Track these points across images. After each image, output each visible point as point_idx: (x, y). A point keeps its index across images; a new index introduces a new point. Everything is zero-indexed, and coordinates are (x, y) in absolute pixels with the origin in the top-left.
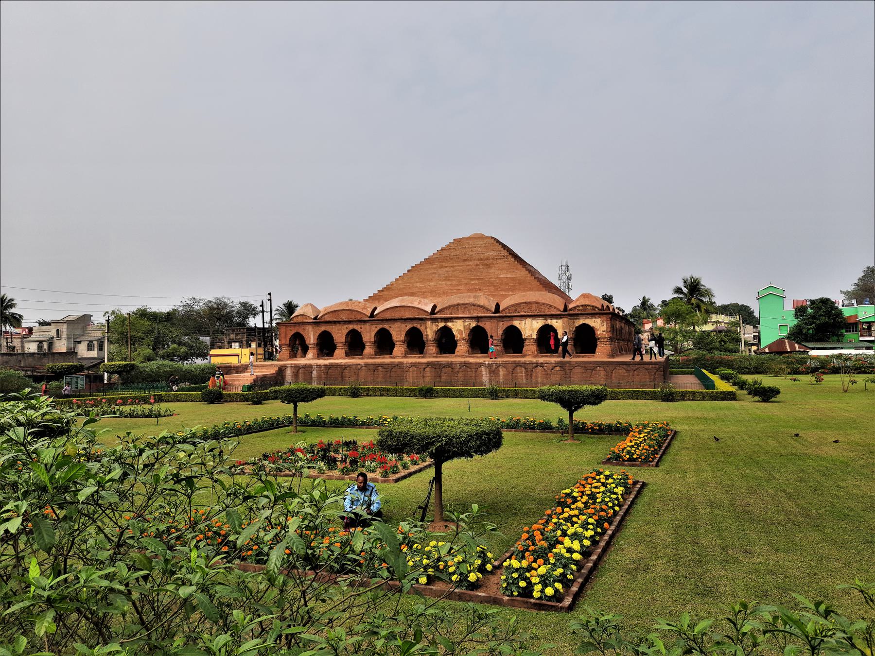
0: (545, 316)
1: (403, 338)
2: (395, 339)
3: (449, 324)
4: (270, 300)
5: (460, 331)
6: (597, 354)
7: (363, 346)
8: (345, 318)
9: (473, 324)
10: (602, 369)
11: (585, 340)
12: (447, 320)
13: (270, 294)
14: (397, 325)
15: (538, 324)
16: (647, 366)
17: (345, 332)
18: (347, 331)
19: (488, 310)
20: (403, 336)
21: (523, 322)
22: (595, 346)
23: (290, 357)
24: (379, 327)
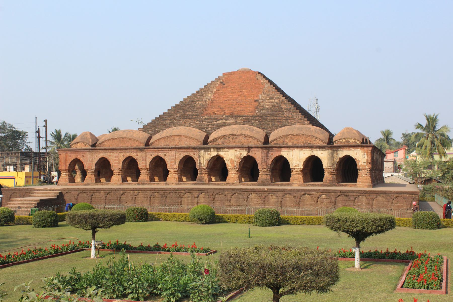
0: (311, 147)
1: (177, 166)
2: (169, 166)
3: (222, 154)
4: (45, 126)
5: (232, 161)
6: (358, 183)
7: (138, 173)
8: (121, 145)
9: (244, 153)
10: (364, 198)
11: (347, 169)
12: (218, 149)
13: (45, 121)
14: (172, 153)
15: (305, 154)
16: (405, 196)
17: (122, 159)
18: (123, 158)
19: (258, 140)
20: (177, 164)
21: (291, 153)
22: (357, 176)
23: (70, 182)
24: (154, 155)
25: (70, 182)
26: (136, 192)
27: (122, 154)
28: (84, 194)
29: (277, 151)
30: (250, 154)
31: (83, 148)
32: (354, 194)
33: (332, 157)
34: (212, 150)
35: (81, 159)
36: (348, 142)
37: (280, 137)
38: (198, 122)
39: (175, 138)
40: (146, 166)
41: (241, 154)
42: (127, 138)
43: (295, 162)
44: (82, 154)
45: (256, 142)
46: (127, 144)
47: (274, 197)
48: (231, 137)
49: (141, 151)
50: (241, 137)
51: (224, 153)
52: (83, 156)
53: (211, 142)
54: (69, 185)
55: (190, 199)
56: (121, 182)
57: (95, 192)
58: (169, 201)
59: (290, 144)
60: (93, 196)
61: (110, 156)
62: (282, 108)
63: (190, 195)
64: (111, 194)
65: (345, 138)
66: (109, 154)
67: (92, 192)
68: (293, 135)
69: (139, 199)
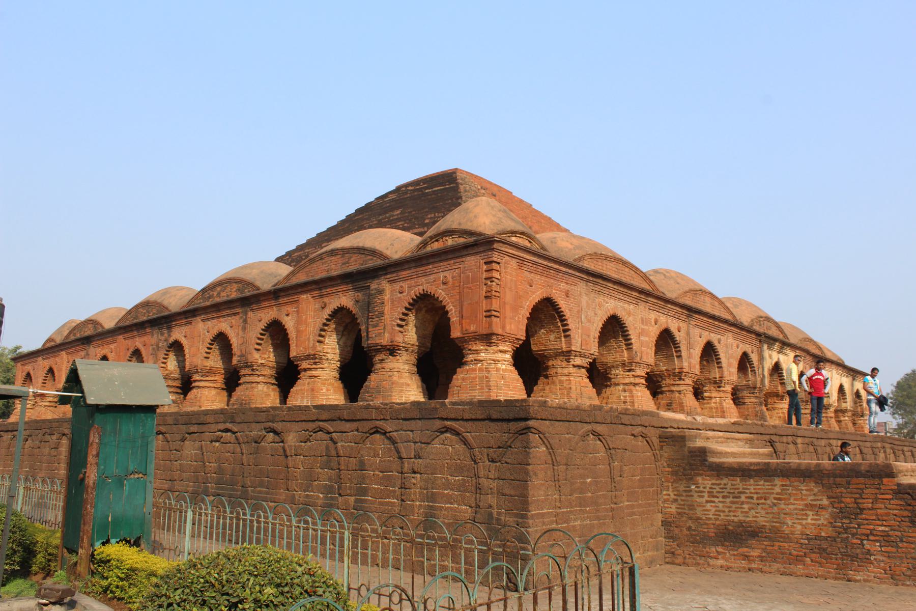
3: (782, 358)
24: (707, 336)
27: (653, 315)
33: (852, 390)
35: (562, 304)
40: (694, 367)
44: (563, 286)
49: (689, 316)
61: (629, 314)
66: (626, 305)
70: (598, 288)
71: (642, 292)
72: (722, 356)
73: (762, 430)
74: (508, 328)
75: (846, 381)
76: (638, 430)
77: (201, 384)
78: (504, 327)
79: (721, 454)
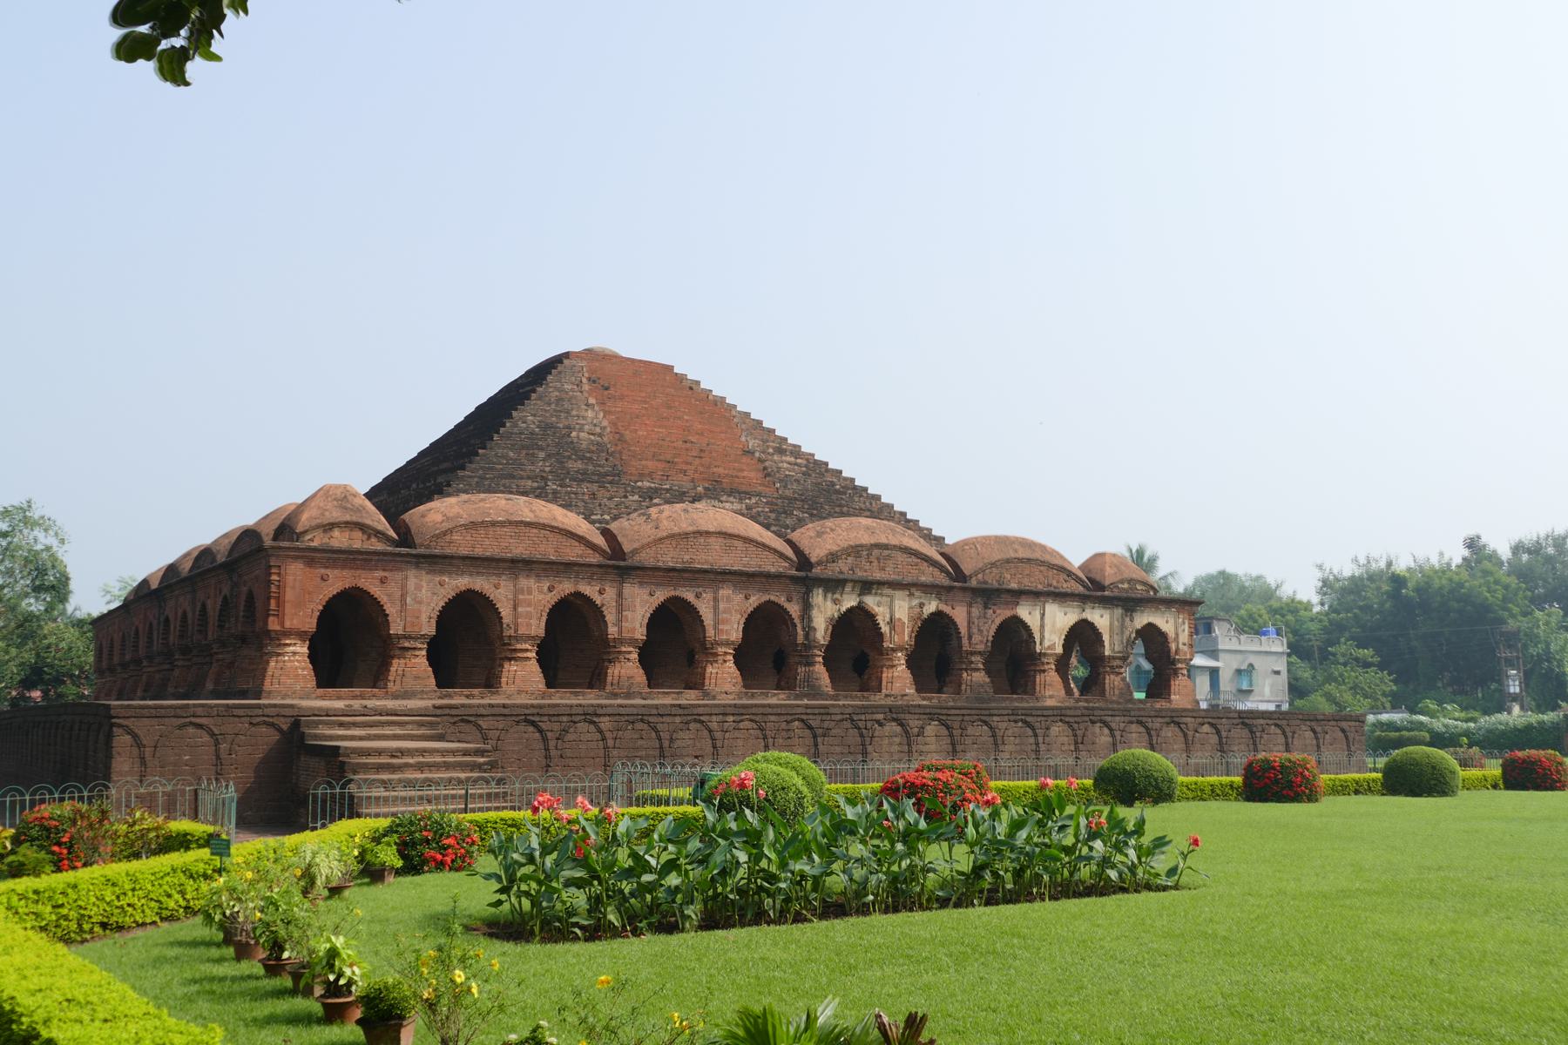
3: (870, 601)
9: (931, 607)
12: (867, 586)
18: (553, 598)
23: (319, 686)
25: (319, 686)
26: (731, 718)
28: (531, 729)
29: (1007, 603)
30: (946, 609)
31: (357, 545)
32: (1262, 721)
33: (1123, 626)
34: (848, 588)
35: (376, 590)
36: (1133, 589)
37: (993, 565)
38: (636, 497)
39: (712, 540)
40: (634, 629)
41: (921, 605)
42: (544, 526)
43: (1047, 635)
45: (937, 572)
46: (542, 548)
47: (1106, 731)
48: (876, 552)
50: (901, 557)
51: (878, 598)
52: (383, 581)
53: (819, 563)
54: (322, 698)
55: (897, 740)
56: (542, 686)
57: (576, 719)
58: (838, 749)
59: (1014, 586)
60: (570, 737)
61: (497, 587)
62: (833, 484)
63: (899, 729)
64: (639, 726)
65: (1130, 581)
66: (494, 580)
67: (565, 719)
68: (1021, 560)
69: (740, 743)
70: (437, 568)
71: (513, 561)
72: (705, 609)
73: (506, 711)
74: (288, 624)
75: (1101, 618)
76: (255, 720)
77: (179, 663)
78: (282, 624)
79: (316, 737)
